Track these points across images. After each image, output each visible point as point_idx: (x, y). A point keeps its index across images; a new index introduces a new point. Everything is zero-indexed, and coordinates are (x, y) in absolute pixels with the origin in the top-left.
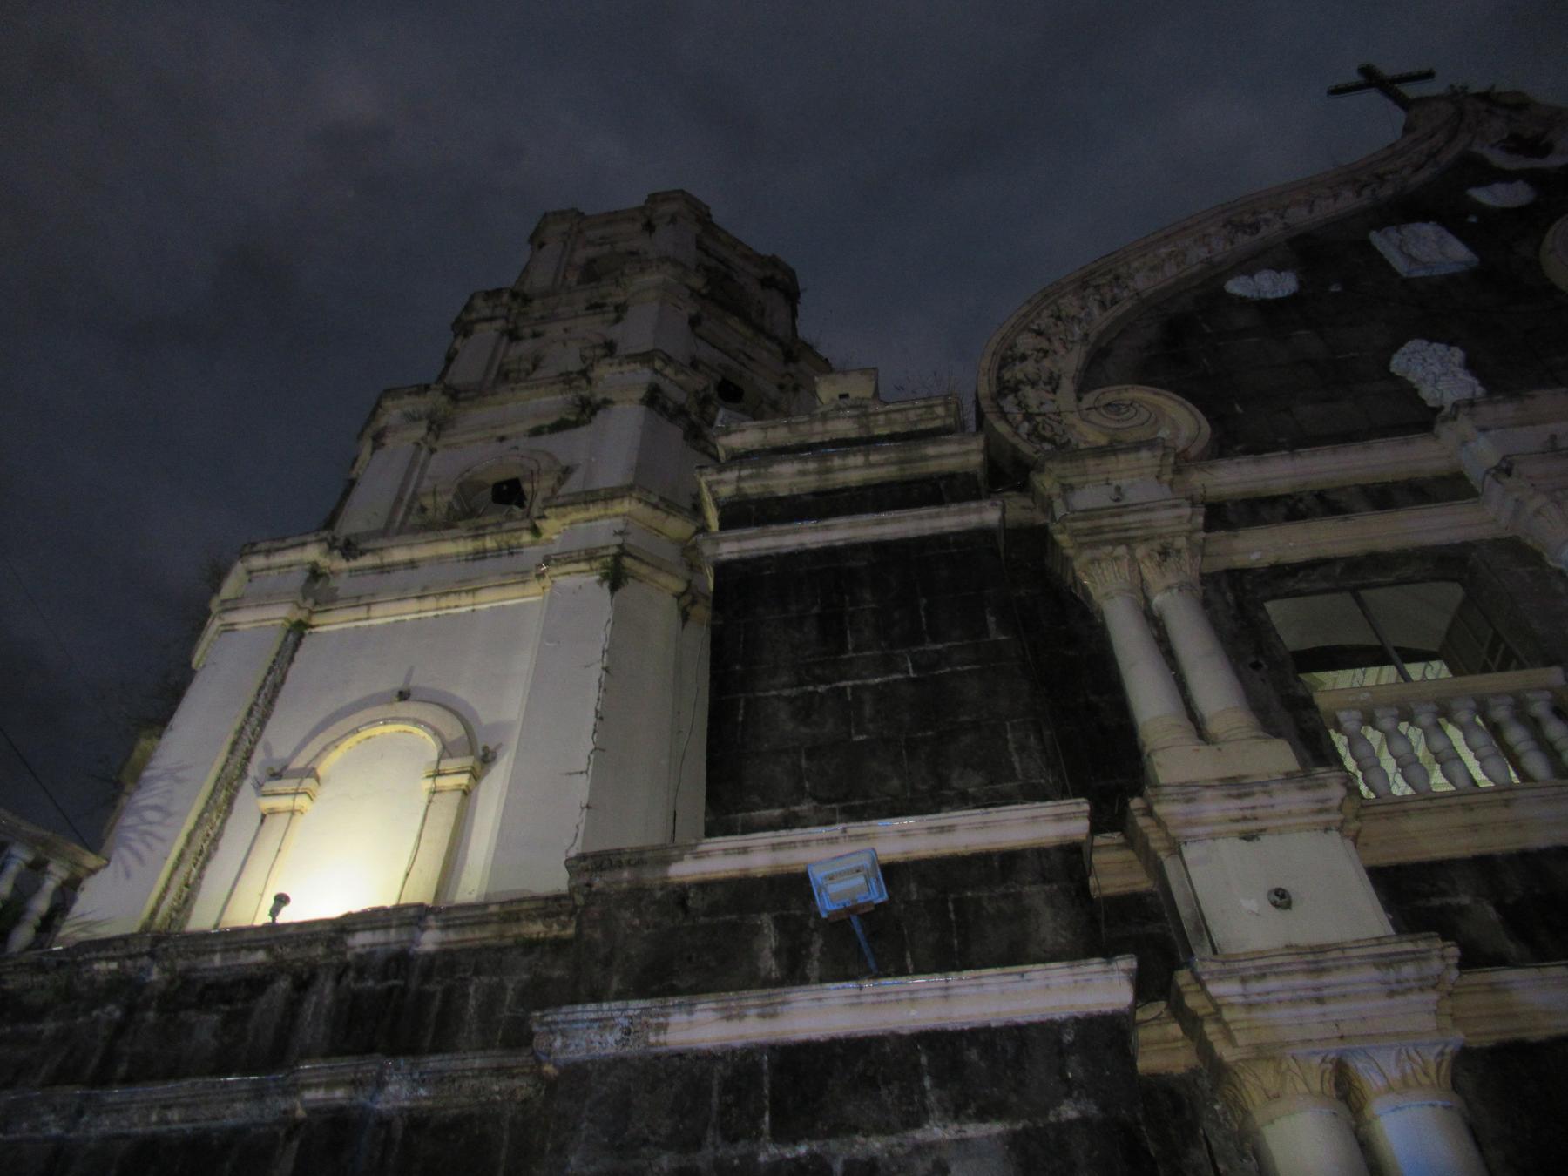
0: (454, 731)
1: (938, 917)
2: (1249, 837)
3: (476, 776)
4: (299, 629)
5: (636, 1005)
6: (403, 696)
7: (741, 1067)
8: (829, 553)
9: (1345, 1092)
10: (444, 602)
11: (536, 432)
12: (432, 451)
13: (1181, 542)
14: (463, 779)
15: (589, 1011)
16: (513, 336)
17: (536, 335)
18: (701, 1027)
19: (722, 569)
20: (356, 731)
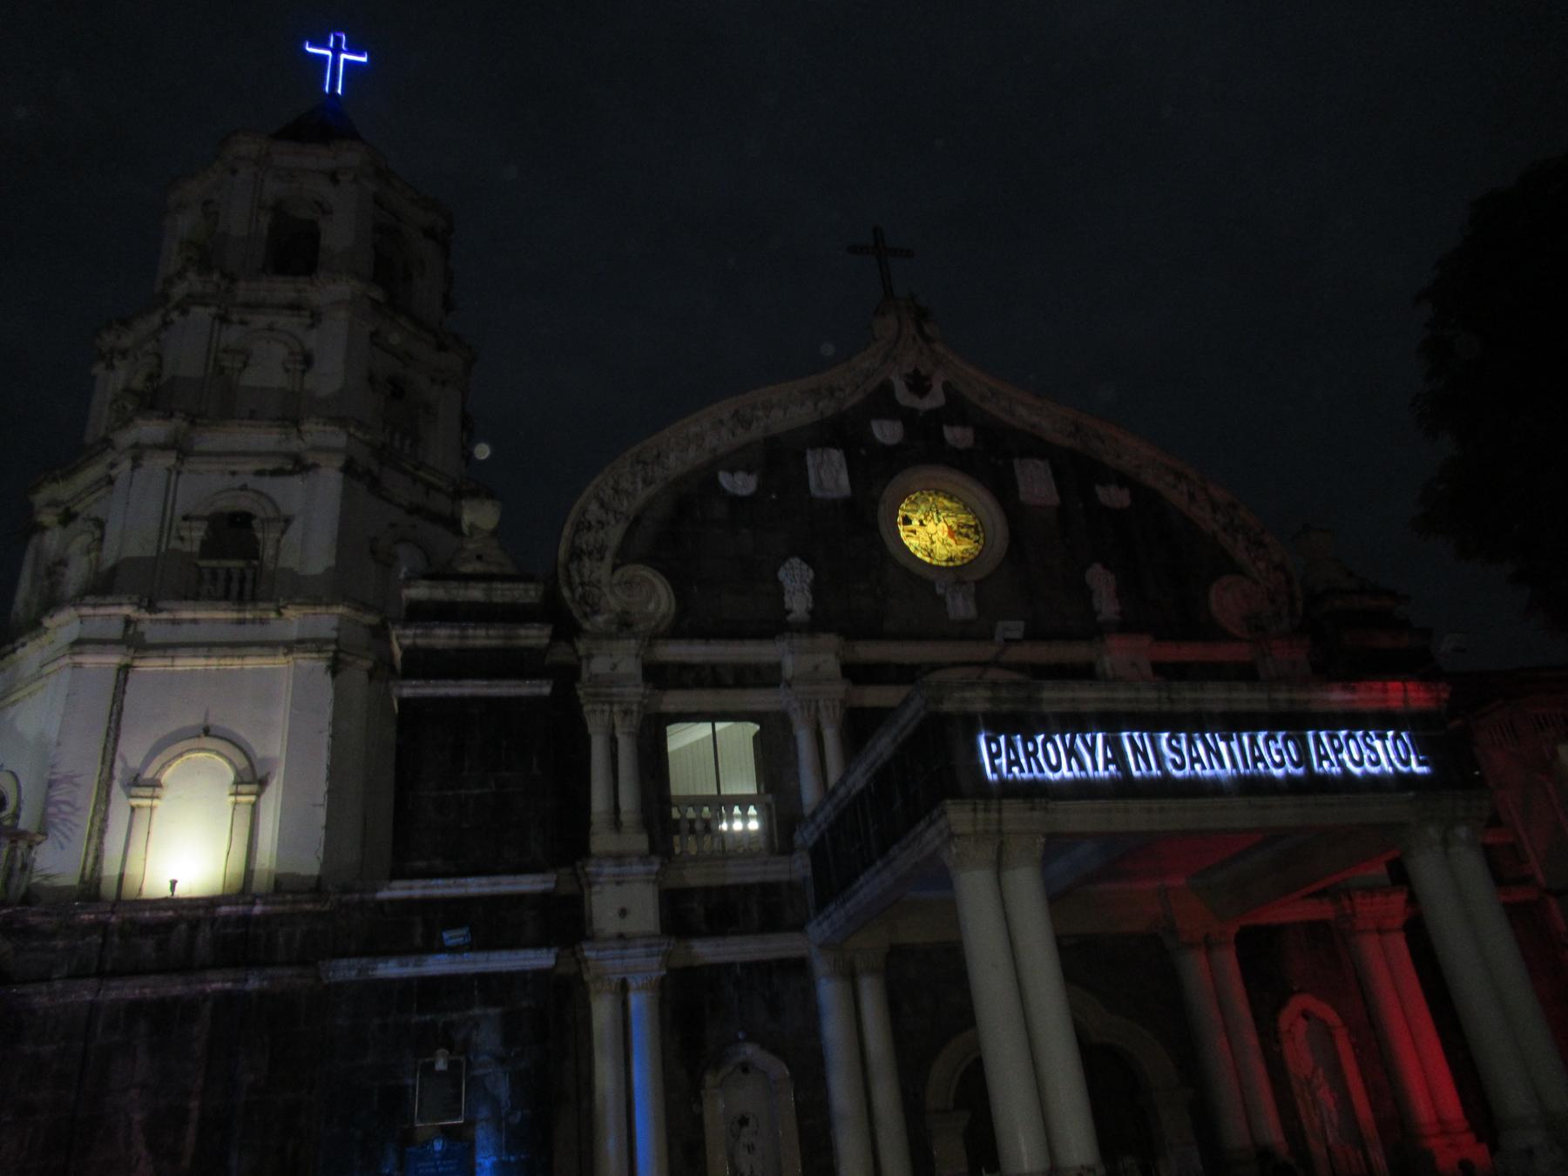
0: (242, 762)
1: (492, 924)
2: (618, 883)
3: (258, 795)
4: (124, 670)
5: (364, 961)
6: (207, 732)
7: (407, 982)
8: (462, 701)
9: (624, 987)
10: (223, 662)
11: (260, 473)
12: (179, 473)
13: (635, 707)
14: (253, 798)
15: (344, 962)
16: (224, 319)
17: (243, 323)
18: (389, 969)
19: (403, 702)
20: (181, 755)
